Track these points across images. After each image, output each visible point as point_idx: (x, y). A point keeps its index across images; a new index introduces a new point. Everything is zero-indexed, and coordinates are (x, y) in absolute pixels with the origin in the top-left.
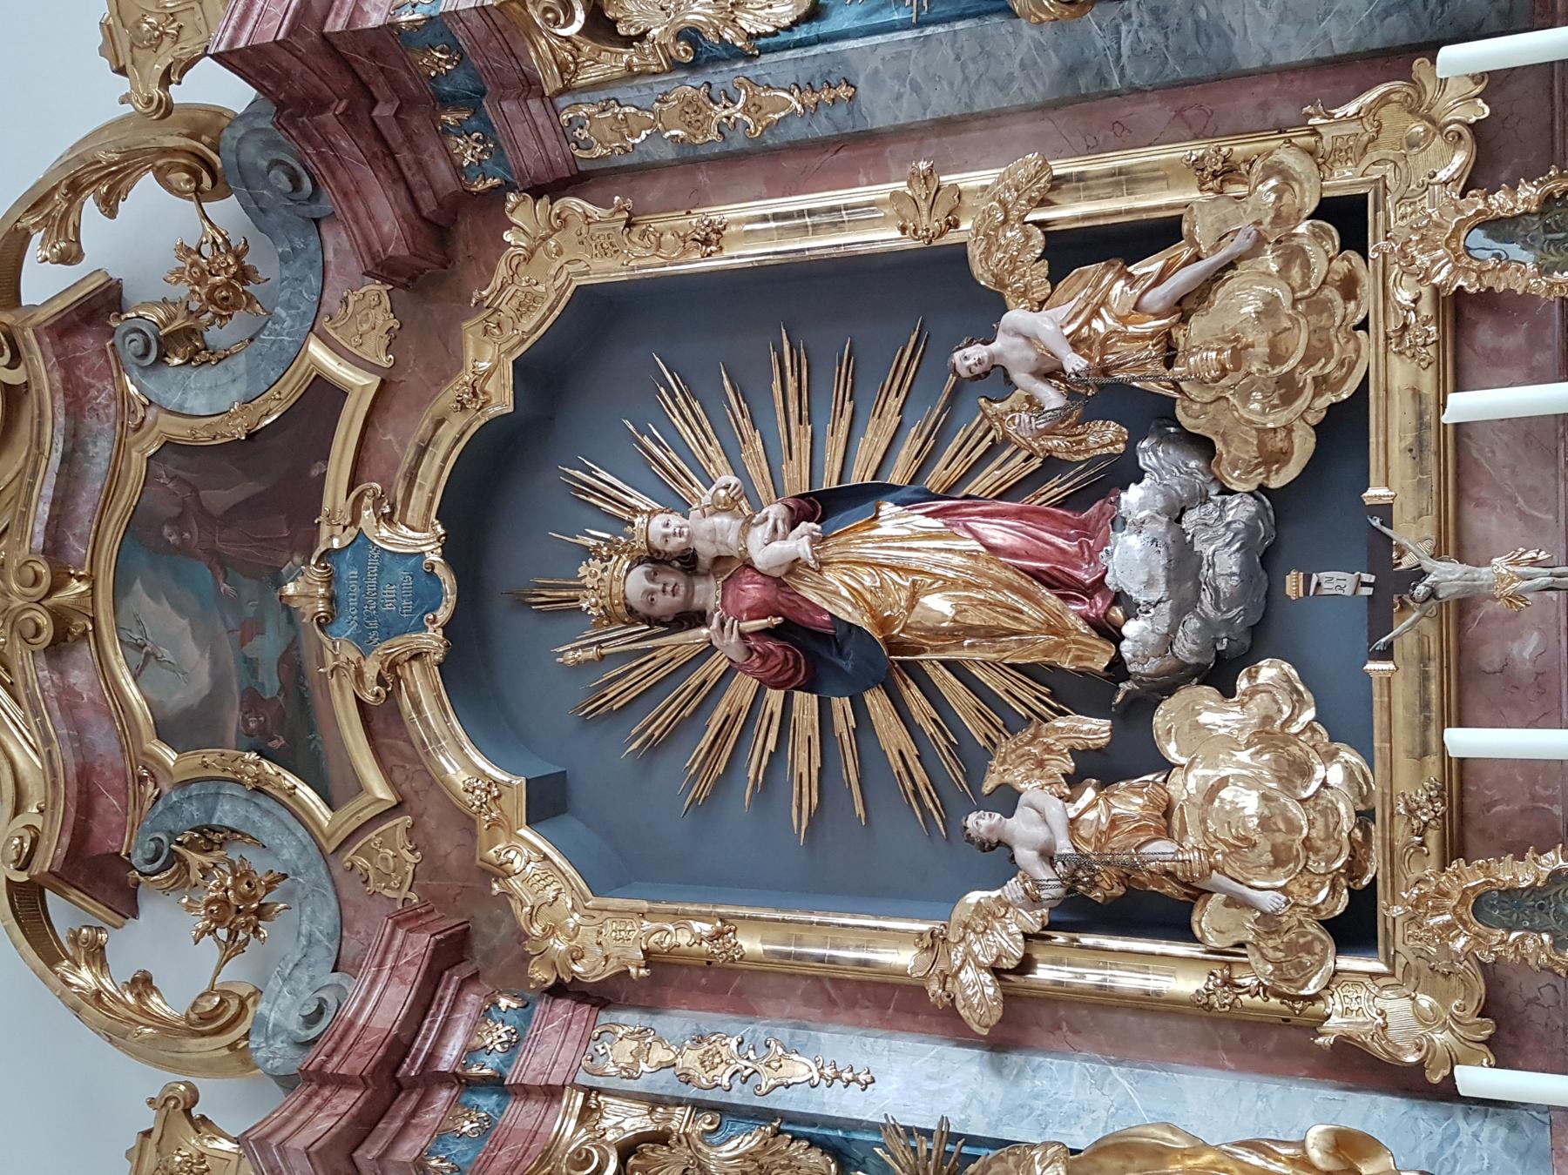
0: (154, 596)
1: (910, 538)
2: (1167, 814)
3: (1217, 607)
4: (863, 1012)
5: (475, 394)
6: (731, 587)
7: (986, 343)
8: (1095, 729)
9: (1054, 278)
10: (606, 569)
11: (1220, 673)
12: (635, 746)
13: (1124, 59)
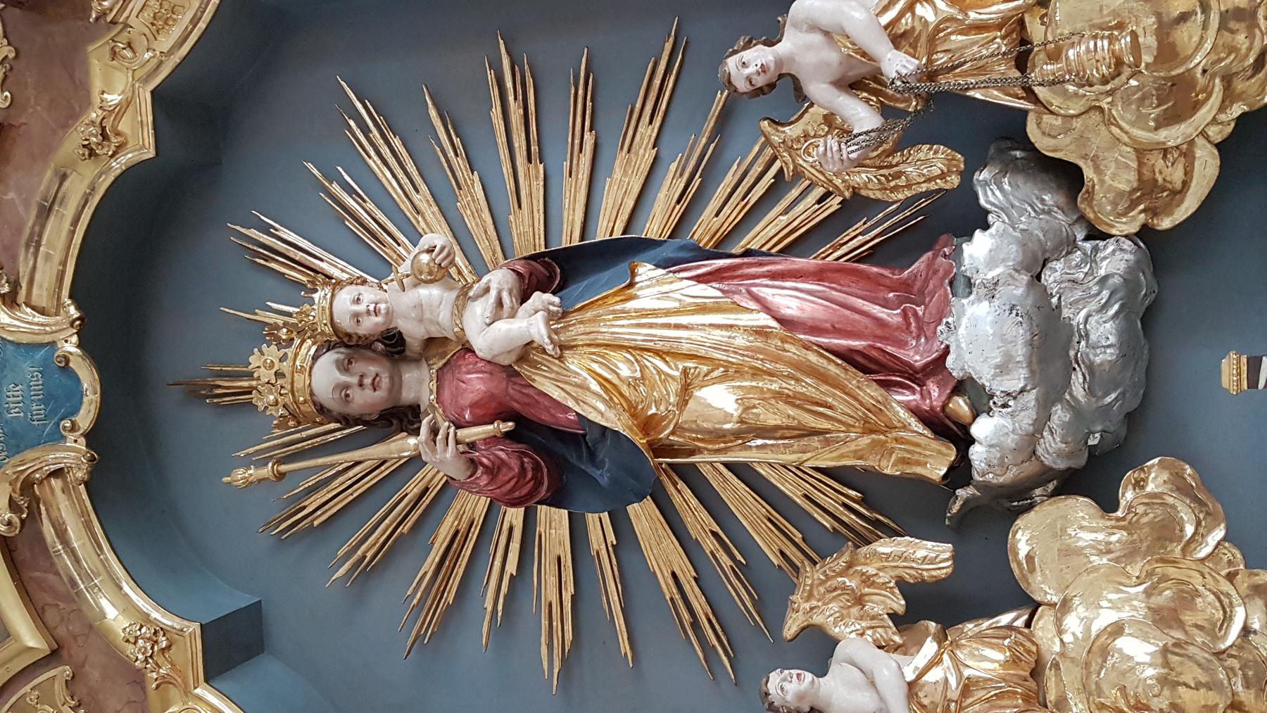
1: (677, 312)
2: (1036, 673)
6: (448, 376)
7: (770, 43)
8: (930, 556)
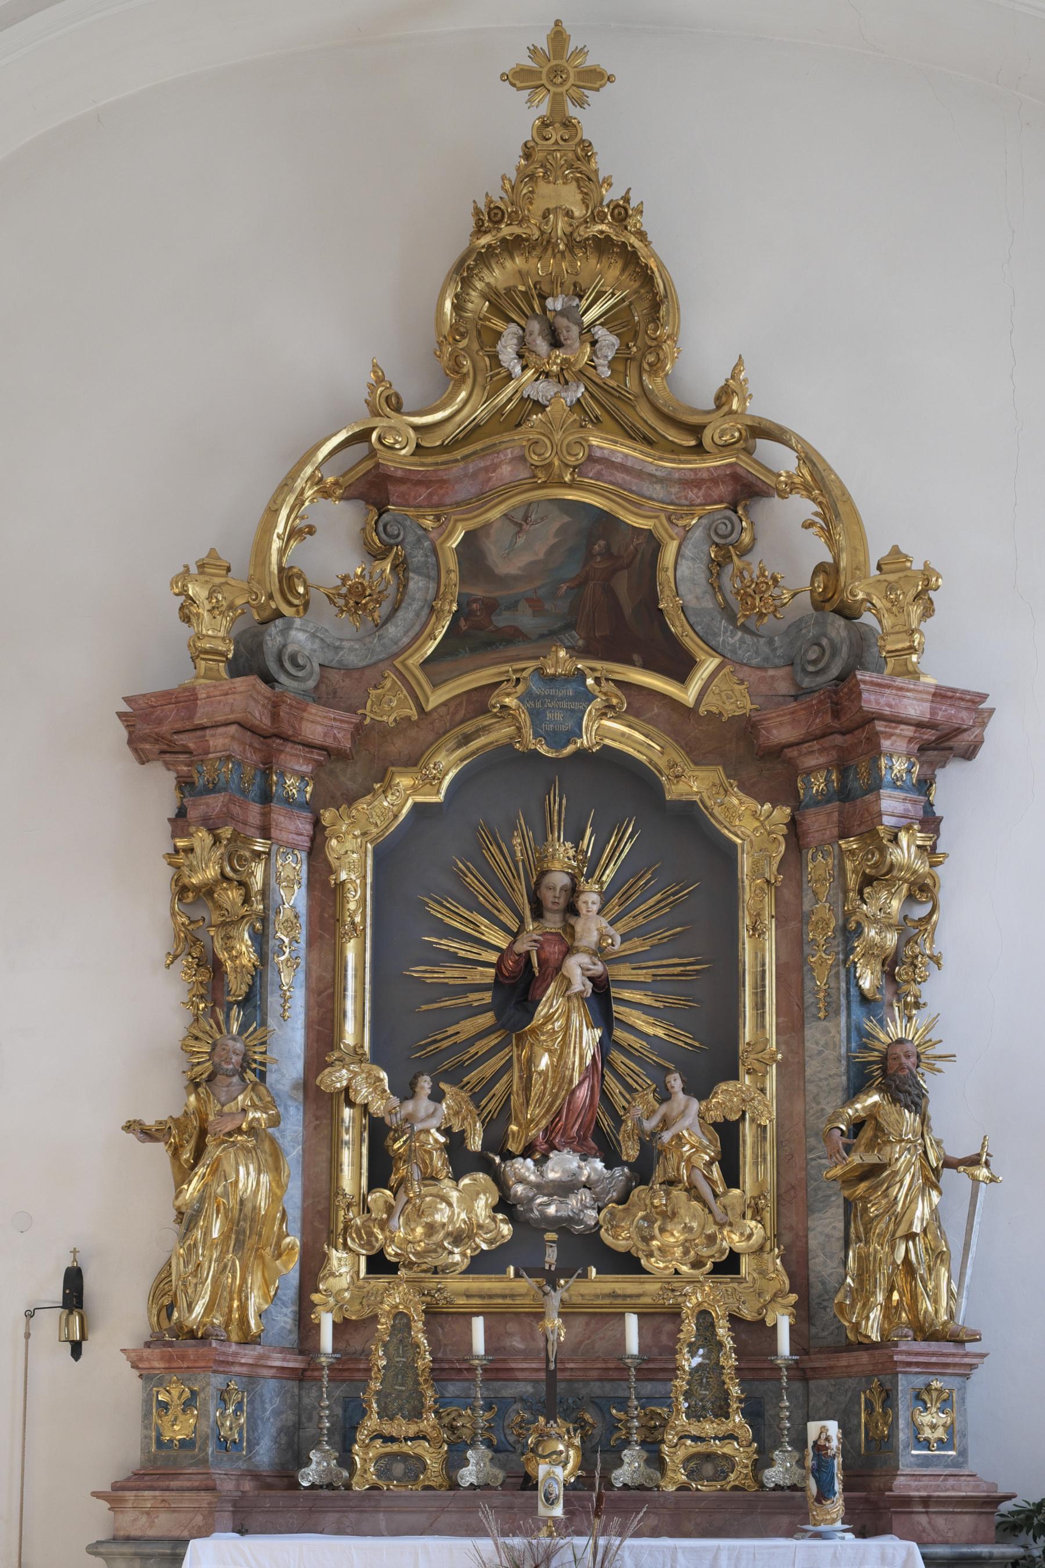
0: (556, 534)
2: (433, 1178)
3: (540, 1204)
4: (315, 1011)
5: (677, 777)
6: (557, 938)
7: (683, 1090)
8: (475, 1143)
9: (715, 1125)
10: (569, 859)
11: (505, 1206)
12: (461, 865)
13: (819, 1161)
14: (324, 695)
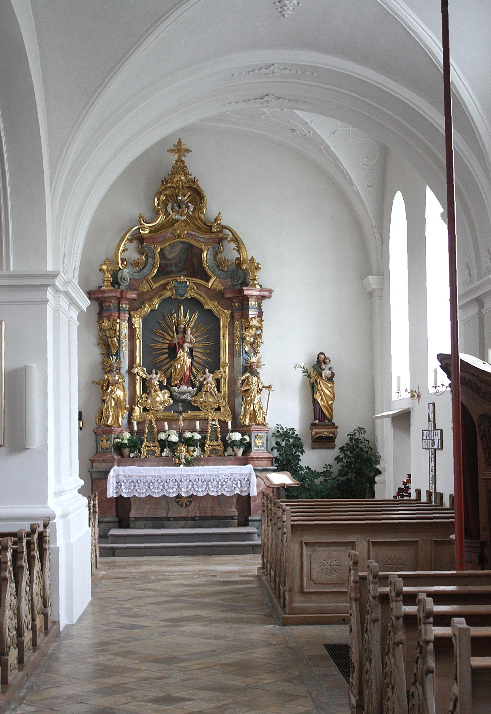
11: (171, 396)
14: (131, 287)
